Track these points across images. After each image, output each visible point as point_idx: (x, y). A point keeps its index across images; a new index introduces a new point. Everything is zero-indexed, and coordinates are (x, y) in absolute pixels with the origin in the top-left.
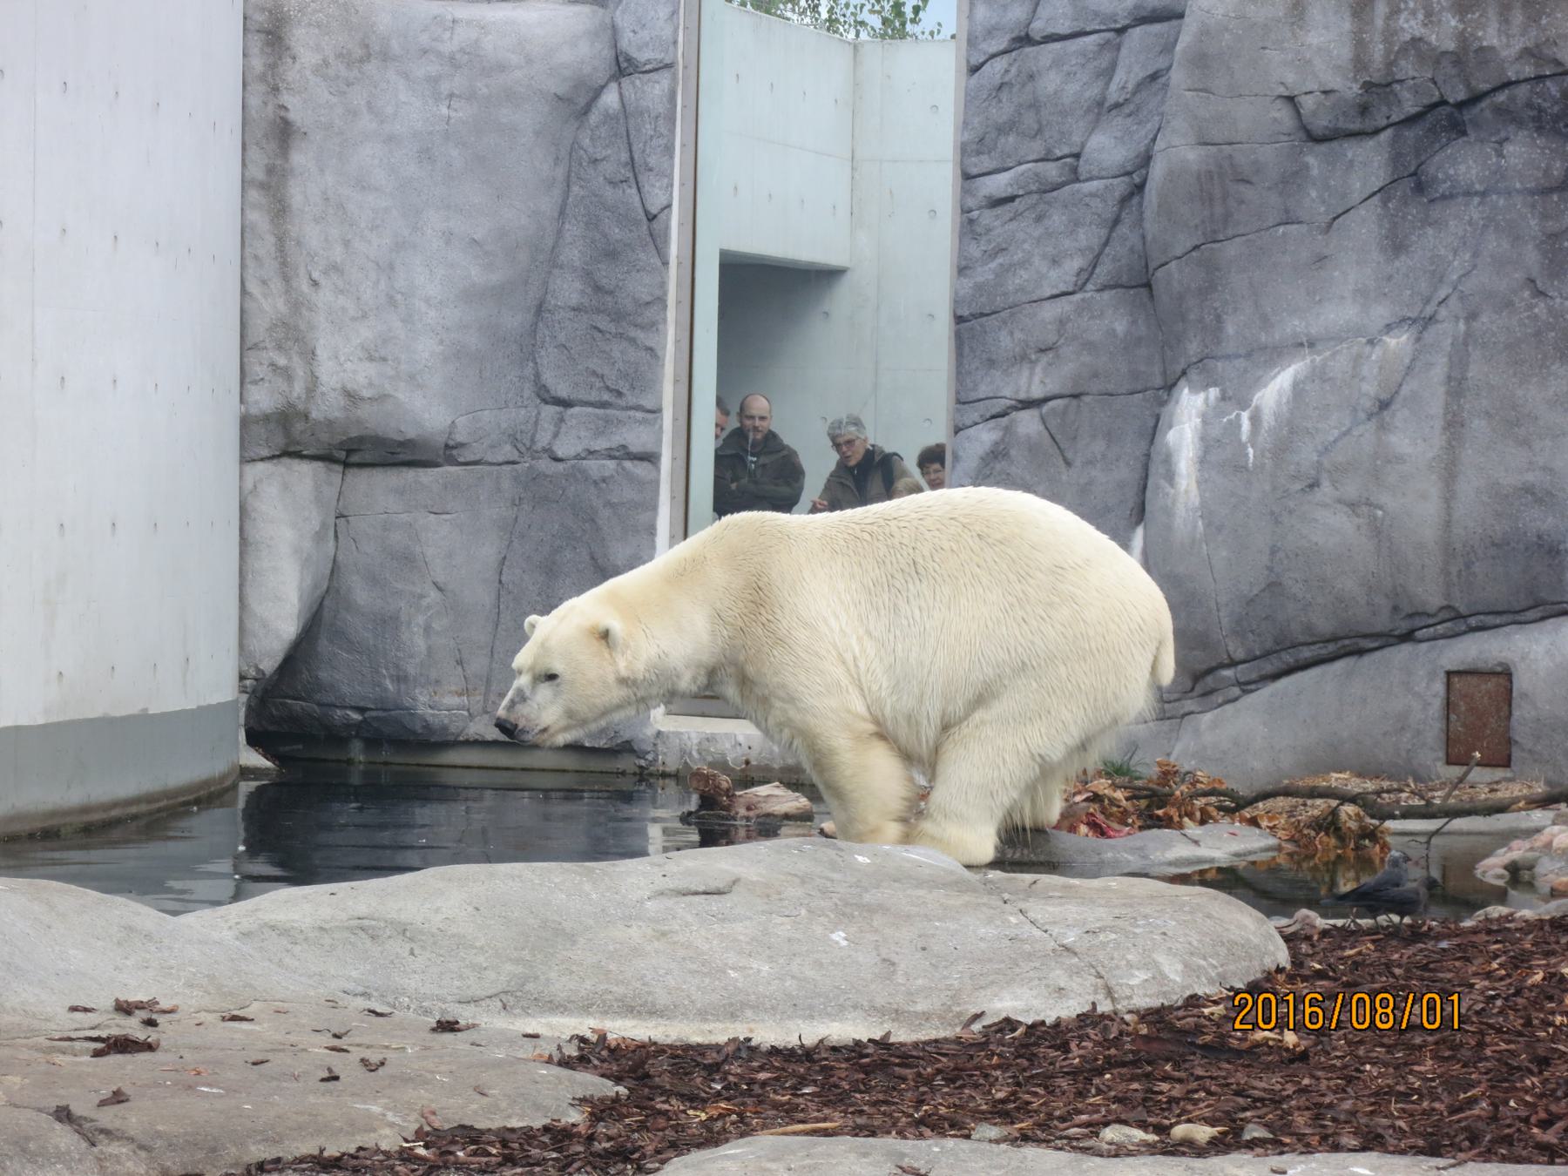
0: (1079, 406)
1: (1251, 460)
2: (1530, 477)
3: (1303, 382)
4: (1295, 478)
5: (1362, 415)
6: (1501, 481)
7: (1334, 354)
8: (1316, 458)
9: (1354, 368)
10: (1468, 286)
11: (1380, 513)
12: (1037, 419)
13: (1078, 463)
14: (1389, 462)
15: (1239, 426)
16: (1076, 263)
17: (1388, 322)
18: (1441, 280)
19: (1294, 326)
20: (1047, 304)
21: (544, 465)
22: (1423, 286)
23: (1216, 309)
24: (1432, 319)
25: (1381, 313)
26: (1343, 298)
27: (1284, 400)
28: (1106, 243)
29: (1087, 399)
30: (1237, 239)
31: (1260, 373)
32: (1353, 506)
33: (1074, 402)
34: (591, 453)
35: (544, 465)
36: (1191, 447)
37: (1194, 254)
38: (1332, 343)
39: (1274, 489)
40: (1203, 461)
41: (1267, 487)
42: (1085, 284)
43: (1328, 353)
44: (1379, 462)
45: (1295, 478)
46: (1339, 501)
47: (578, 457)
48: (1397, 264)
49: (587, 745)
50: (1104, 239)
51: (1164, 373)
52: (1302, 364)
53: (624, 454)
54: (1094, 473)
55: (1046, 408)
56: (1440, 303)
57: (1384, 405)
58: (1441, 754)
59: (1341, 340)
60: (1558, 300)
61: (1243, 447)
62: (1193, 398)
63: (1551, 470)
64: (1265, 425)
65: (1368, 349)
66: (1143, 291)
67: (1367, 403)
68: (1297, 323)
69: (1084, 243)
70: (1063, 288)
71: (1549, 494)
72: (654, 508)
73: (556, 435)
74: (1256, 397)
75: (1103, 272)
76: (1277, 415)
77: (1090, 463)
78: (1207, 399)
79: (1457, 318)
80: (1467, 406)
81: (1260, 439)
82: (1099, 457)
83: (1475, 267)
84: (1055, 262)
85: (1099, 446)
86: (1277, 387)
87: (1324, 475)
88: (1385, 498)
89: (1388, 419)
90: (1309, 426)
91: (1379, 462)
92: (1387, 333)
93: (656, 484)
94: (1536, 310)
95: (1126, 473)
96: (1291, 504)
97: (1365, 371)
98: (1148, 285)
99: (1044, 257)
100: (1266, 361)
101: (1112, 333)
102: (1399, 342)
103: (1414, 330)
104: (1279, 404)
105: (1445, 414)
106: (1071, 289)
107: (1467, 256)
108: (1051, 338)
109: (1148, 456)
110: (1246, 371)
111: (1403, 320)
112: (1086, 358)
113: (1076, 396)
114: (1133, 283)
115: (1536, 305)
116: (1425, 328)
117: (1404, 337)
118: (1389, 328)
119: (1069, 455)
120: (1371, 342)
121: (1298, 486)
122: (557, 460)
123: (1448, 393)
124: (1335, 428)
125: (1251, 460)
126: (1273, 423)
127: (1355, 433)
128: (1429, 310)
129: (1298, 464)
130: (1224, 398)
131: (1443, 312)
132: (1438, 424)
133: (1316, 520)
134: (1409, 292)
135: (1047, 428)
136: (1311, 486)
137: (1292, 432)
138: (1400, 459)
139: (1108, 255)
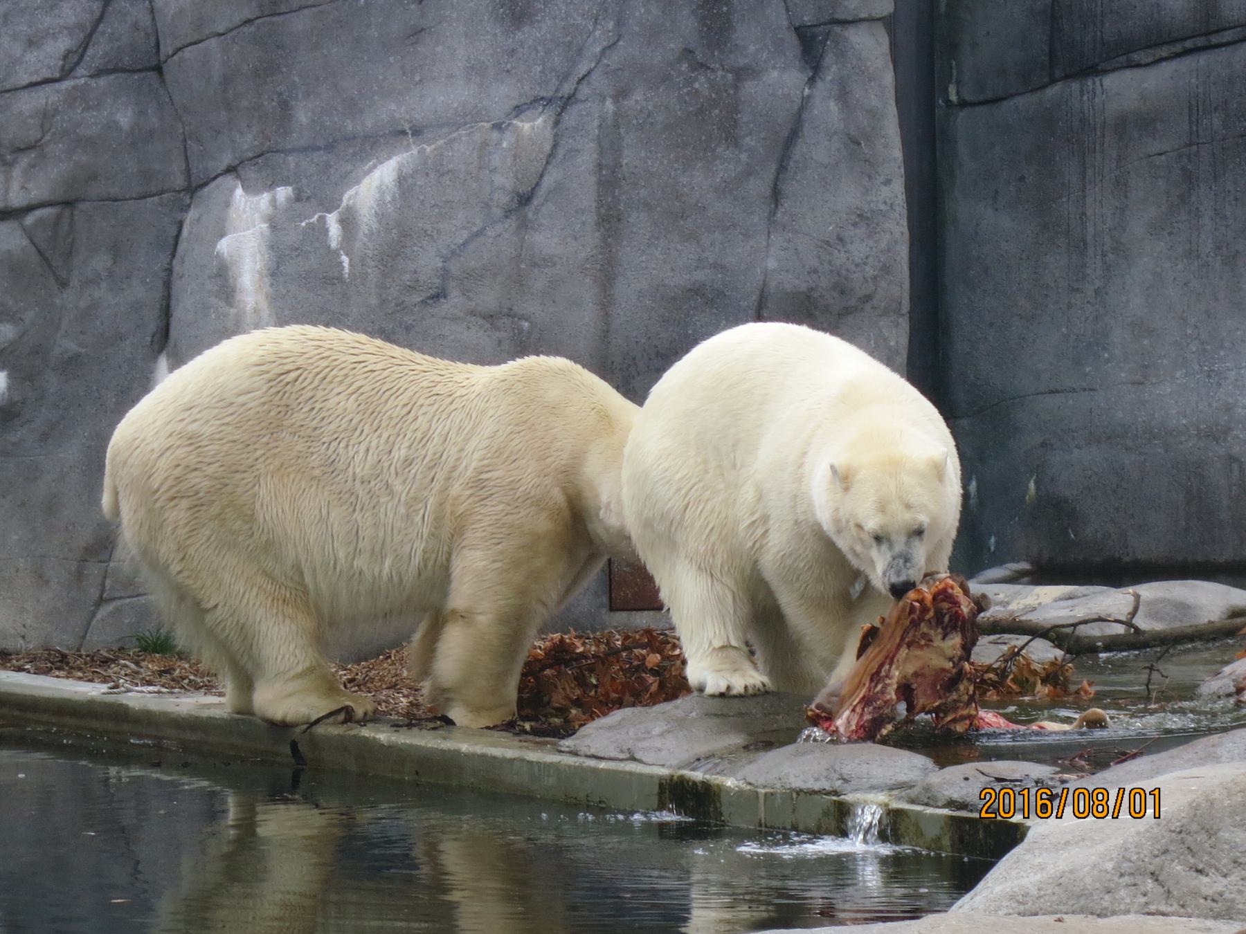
0: (72, 214)
1: (347, 270)
2: (700, 276)
3: (412, 176)
4: (411, 289)
5: (498, 212)
6: (666, 282)
7: (450, 143)
8: (440, 265)
9: (480, 157)
10: (614, 59)
11: (526, 324)
12: (19, 232)
13: (75, 282)
14: (535, 265)
15: (327, 231)
16: (64, 43)
17: (516, 103)
18: (580, 50)
19: (389, 110)
20: (24, 95)
22: (557, 60)
23: (280, 94)
24: (570, 100)
25: (502, 94)
26: (452, 76)
27: (388, 198)
28: (100, 20)
29: (83, 206)
30: (306, 11)
31: (349, 167)
32: (490, 317)
33: (67, 212)
36: (258, 257)
37: (247, 29)
38: (446, 130)
39: (384, 302)
40: (275, 273)
41: (374, 301)
42: (72, 69)
43: (441, 142)
44: (523, 266)
45: (411, 289)
46: (472, 313)
48: (519, 35)
50: (98, 14)
51: (188, 172)
52: (405, 155)
54: (97, 294)
55: (30, 220)
56: (580, 81)
57: (524, 200)
58: (605, 600)
59: (458, 126)
60: (720, 73)
61: (333, 255)
62: (255, 199)
63: (723, 267)
64: (364, 229)
65: (495, 135)
66: (152, 75)
67: (503, 199)
68: (393, 107)
69: (72, 20)
70: (46, 74)
71: (721, 294)
74: (346, 197)
75: (97, 53)
76: (380, 216)
77: (93, 281)
78: (273, 201)
79: (603, 98)
80: (624, 197)
81: (358, 245)
82: (104, 274)
83: (620, 37)
84: (32, 43)
85: (101, 262)
86: (375, 184)
87: (452, 283)
88: (531, 307)
89: (530, 215)
90: (428, 227)
91: (523, 266)
92: (516, 116)
94: (697, 85)
95: (142, 291)
96: (408, 319)
97: (496, 161)
98: (158, 69)
99: (14, 37)
100: (354, 154)
101: (112, 126)
102: (534, 126)
103: (551, 112)
104: (381, 203)
105: (598, 208)
106: (57, 75)
107: (611, 25)
108: (34, 134)
109: (169, 270)
110: (328, 166)
111: (536, 100)
112: (81, 157)
113: (68, 204)
114: (139, 67)
115: (696, 79)
116: (564, 108)
117: (540, 121)
118: (518, 110)
119: (63, 274)
120: (498, 127)
121: (417, 298)
123: (600, 183)
124: (463, 228)
125: (347, 270)
126: (375, 226)
127: (490, 233)
128: (567, 88)
129: (415, 272)
130: (298, 198)
131: (585, 90)
132: (591, 218)
133: (442, 336)
134: (539, 68)
135: (32, 242)
136: (439, 296)
137: (405, 234)
138: (549, 261)
139: (103, 33)
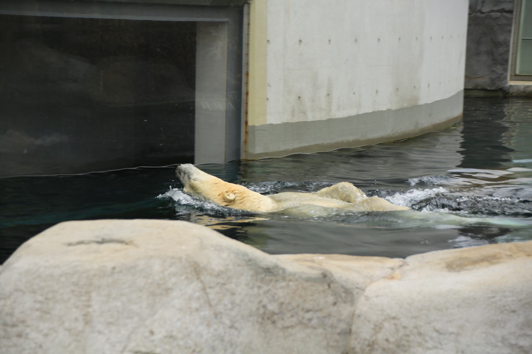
21: (479, 14)
34: (492, 11)
35: (479, 14)
47: (489, 12)
49: (489, 89)
53: (503, 11)
72: (511, 25)
73: (482, 6)
93: (512, 19)
122: (483, 13)
